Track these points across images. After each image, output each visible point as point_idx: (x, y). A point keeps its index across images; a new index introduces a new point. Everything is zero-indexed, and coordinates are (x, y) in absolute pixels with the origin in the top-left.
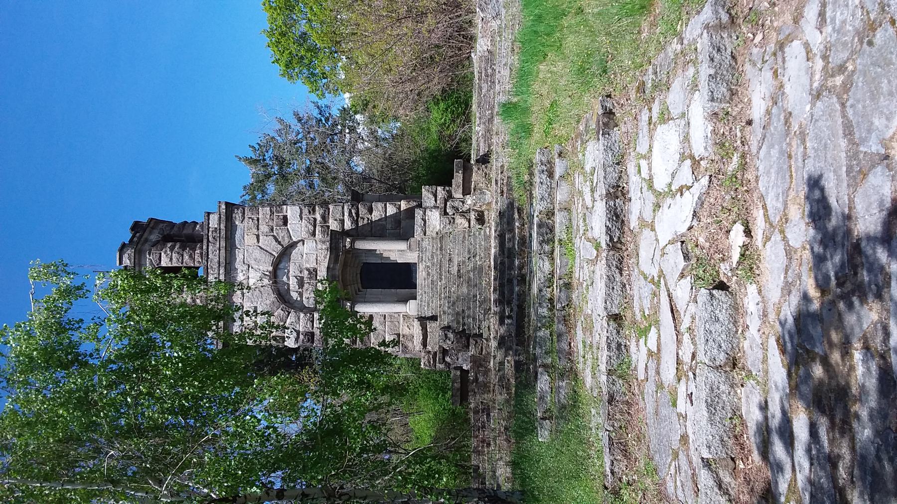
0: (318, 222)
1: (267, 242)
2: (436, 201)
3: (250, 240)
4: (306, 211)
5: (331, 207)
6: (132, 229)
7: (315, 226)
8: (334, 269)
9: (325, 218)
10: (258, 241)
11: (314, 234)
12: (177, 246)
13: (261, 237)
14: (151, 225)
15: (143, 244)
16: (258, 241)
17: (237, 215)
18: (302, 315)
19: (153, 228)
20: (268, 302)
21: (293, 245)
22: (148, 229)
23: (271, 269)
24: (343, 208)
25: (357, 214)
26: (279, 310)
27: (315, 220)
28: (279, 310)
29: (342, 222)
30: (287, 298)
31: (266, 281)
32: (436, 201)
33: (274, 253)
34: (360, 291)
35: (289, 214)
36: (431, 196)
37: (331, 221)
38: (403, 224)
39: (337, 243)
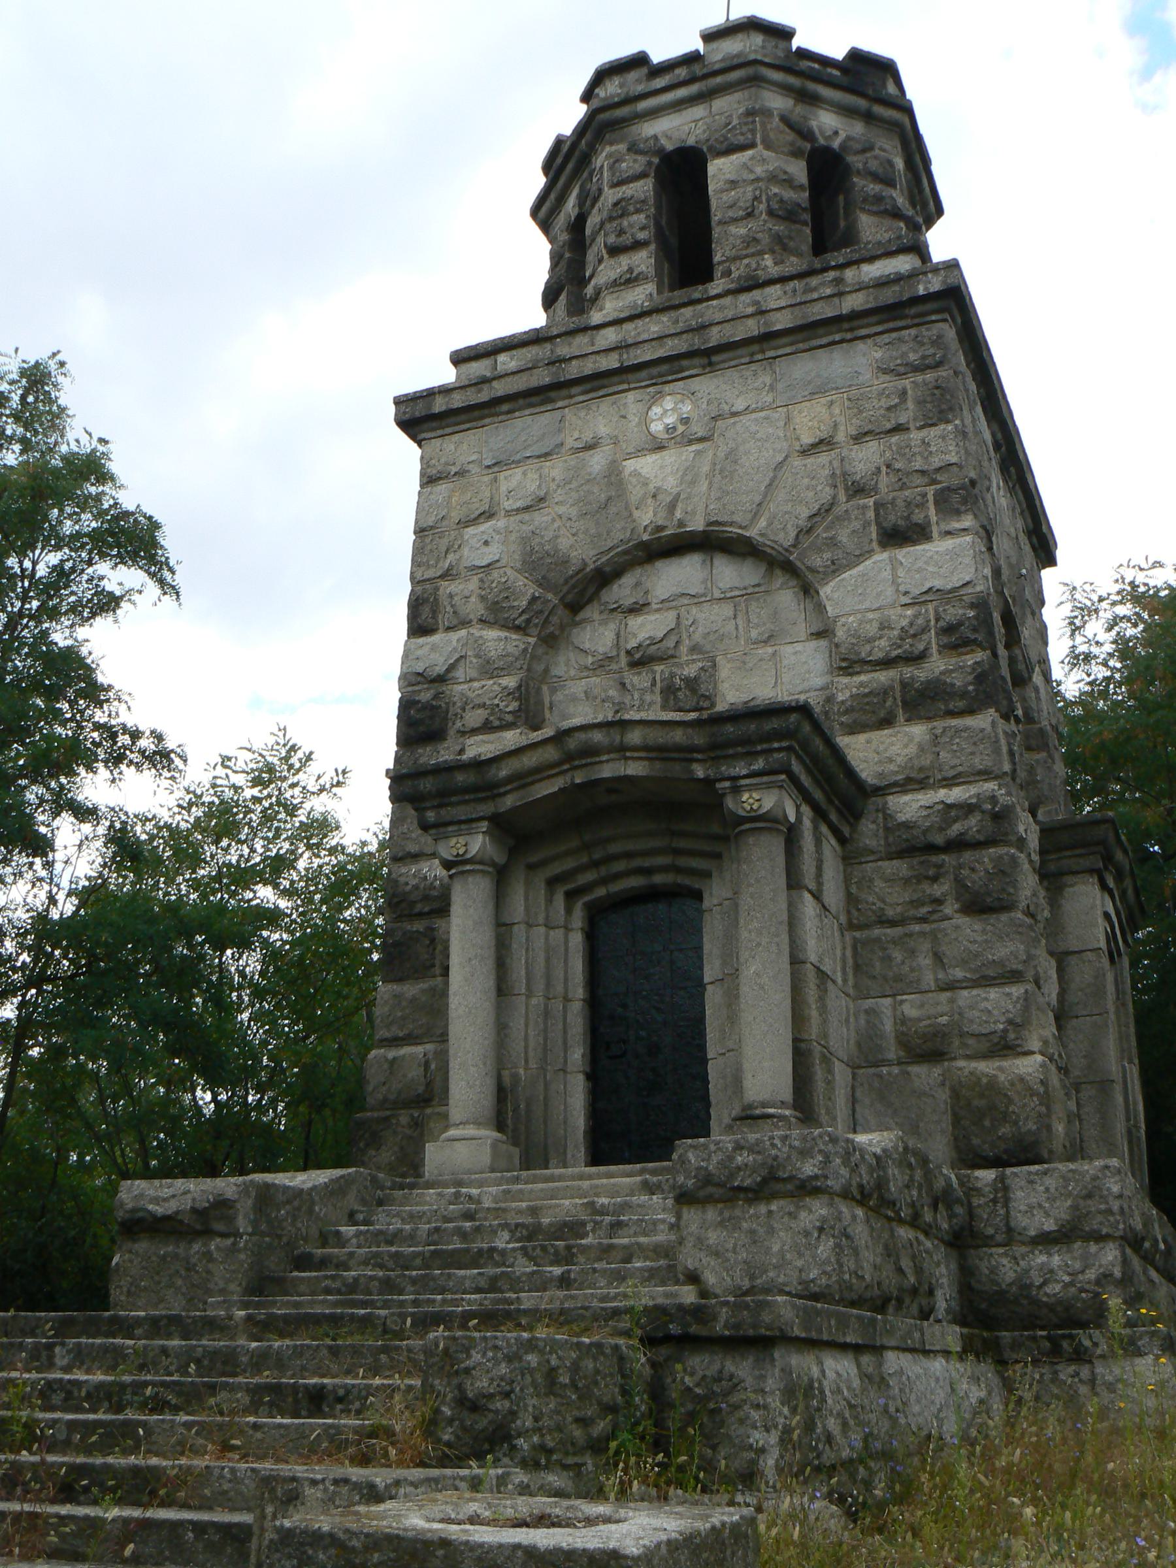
0: (908, 671)
1: (809, 486)
2: (1045, 1240)
3: (810, 421)
4: (953, 613)
5: (984, 720)
6: (856, 56)
7: (887, 663)
8: (622, 750)
9: (922, 701)
10: (805, 452)
11: (849, 665)
12: (789, 194)
13: (823, 458)
14: (878, 109)
15: (786, 89)
16: (805, 452)
17: (908, 344)
18: (511, 682)
19: (868, 118)
20: (564, 543)
21: (807, 590)
22: (862, 103)
23: (697, 524)
24: (985, 774)
25: (958, 845)
26: (532, 590)
27: (918, 658)
28: (532, 590)
29: (915, 782)
30: (591, 612)
31: (646, 517)
32: (1045, 1240)
33: (762, 523)
34: (571, 896)
35: (938, 547)
36: (1062, 1210)
37: (918, 730)
38: (925, 1075)
39: (747, 747)
